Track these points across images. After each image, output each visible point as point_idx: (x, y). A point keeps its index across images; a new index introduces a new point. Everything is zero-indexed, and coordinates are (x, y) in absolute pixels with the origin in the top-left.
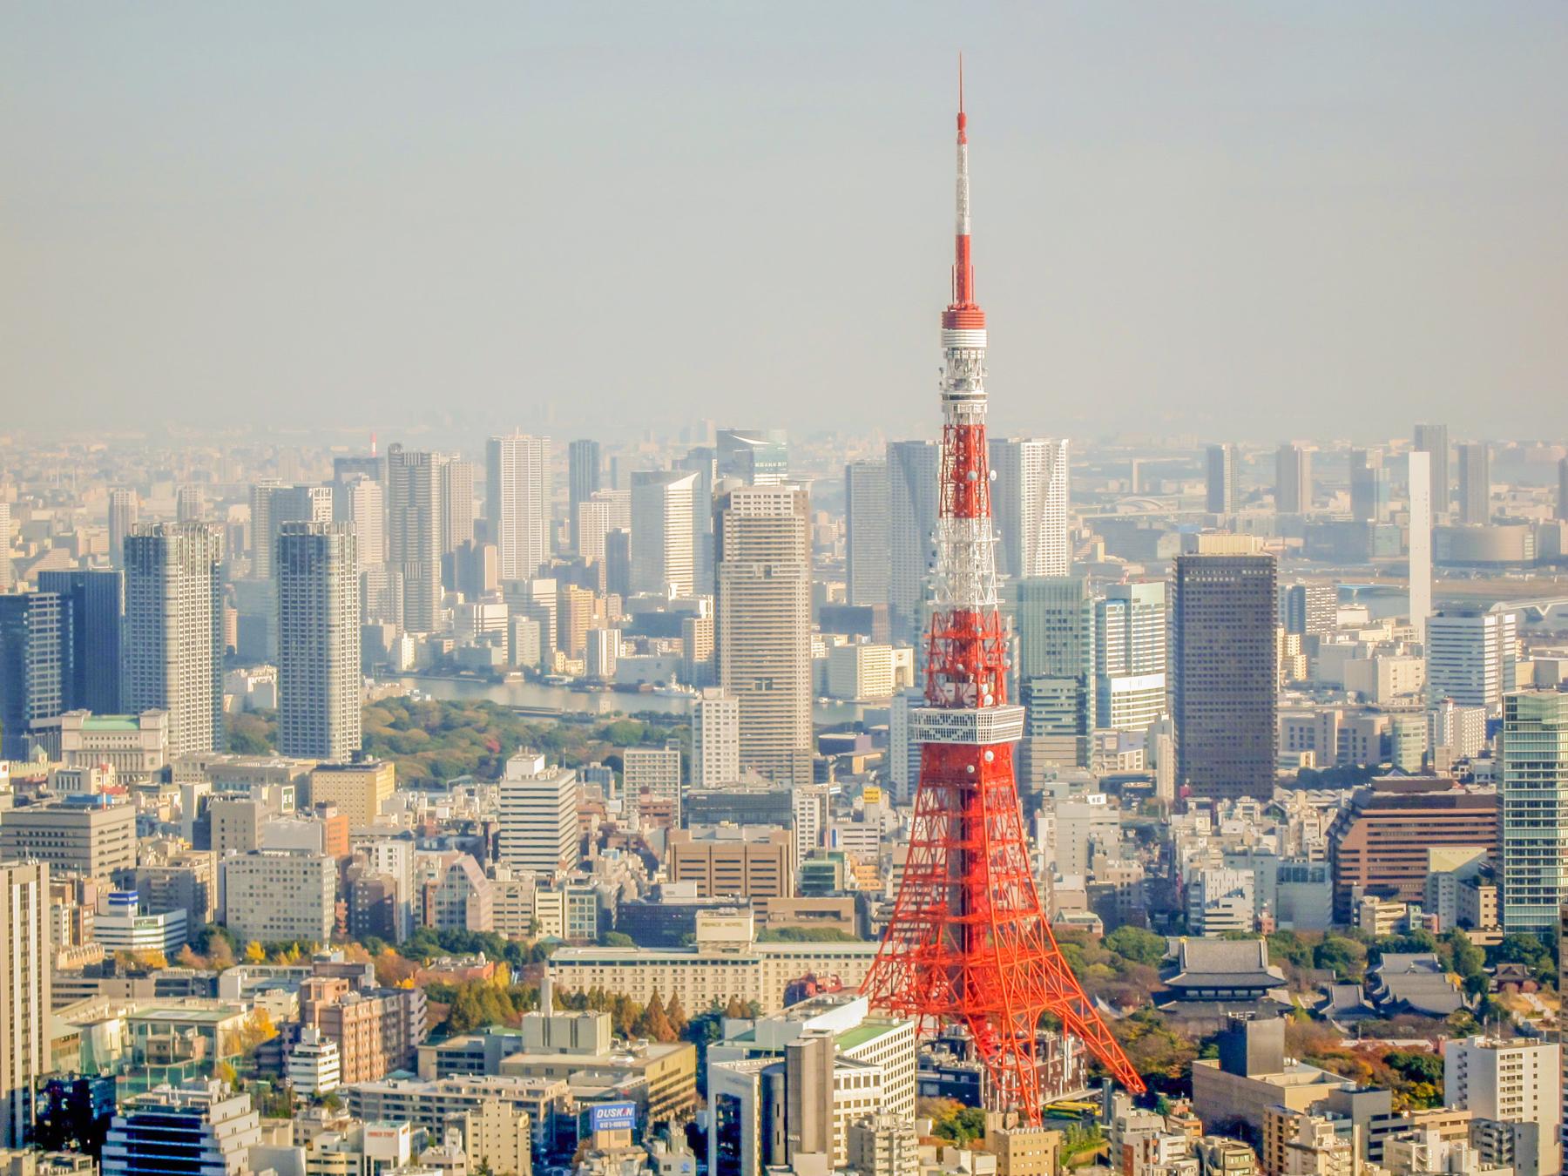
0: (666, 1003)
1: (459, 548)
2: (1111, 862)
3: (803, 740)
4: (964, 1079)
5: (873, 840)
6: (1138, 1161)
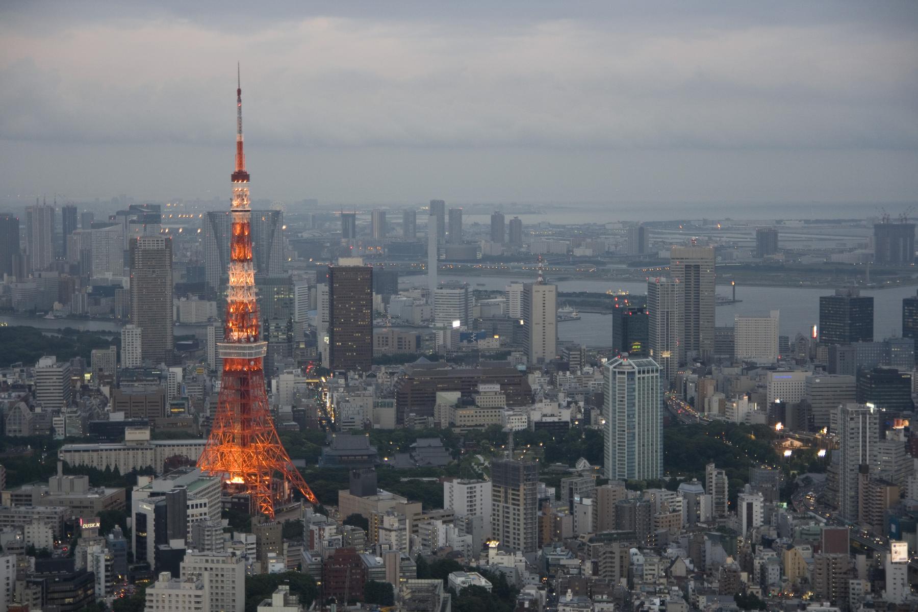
0: (112, 468)
2: (303, 400)
4: (242, 501)
5: (201, 390)
6: (316, 536)
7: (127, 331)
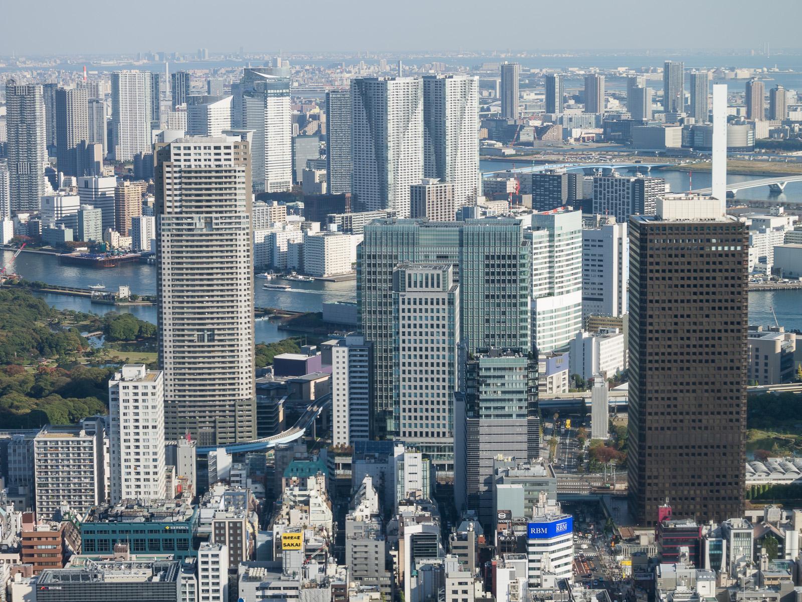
1: (78, 145)
3: (246, 390)
7: (122, 384)
